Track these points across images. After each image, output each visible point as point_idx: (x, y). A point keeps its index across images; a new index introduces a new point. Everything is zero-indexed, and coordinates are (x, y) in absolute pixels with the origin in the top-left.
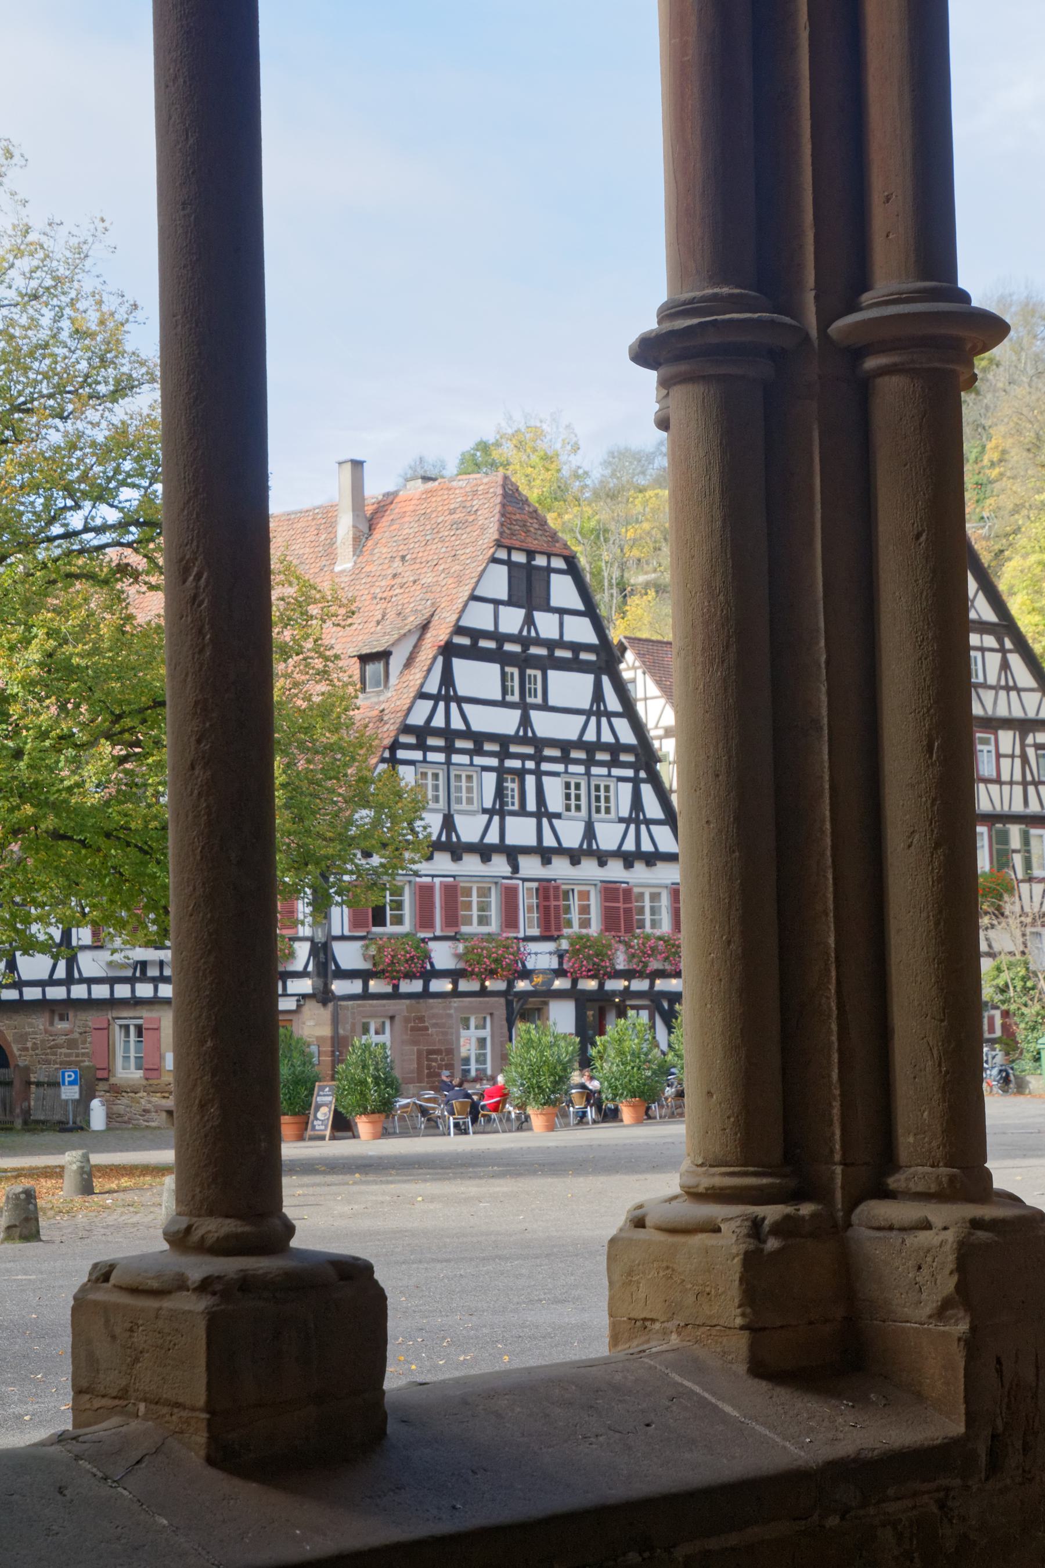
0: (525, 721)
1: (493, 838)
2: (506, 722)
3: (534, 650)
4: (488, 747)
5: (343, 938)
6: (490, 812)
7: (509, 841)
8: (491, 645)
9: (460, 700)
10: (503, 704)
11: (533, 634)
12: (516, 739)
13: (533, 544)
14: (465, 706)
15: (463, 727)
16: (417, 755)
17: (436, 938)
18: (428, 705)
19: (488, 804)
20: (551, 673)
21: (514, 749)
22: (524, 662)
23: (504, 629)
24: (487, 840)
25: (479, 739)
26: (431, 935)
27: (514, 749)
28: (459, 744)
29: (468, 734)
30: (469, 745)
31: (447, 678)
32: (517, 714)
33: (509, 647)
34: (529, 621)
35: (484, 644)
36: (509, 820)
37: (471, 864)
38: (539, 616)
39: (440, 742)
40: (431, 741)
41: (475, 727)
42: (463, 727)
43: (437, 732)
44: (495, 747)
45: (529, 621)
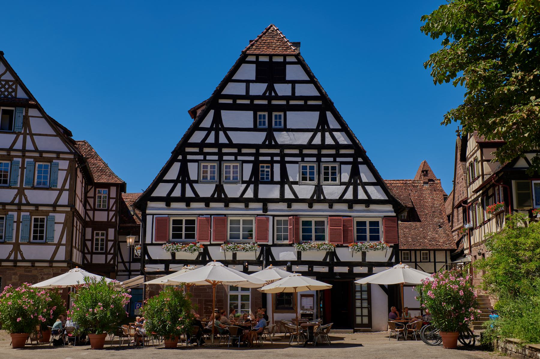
0: (270, 137)
1: (249, 194)
2: (259, 138)
3: (274, 102)
4: (244, 151)
5: (152, 244)
6: (248, 183)
7: (260, 196)
8: (248, 102)
9: (225, 130)
10: (255, 129)
11: (273, 94)
12: (263, 146)
13: (270, 51)
14: (229, 133)
15: (227, 142)
16: (201, 157)
17: (211, 245)
18: (204, 133)
19: (246, 177)
20: (288, 113)
21: (262, 151)
22: (270, 109)
23: (252, 93)
24: (245, 196)
25: (240, 146)
26: (209, 243)
27: (262, 151)
28: (225, 150)
29: (231, 145)
30: (235, 150)
31: (217, 119)
32: (264, 134)
33: (256, 102)
34: (271, 88)
35: (239, 102)
36: (261, 187)
37: (237, 209)
38: (277, 86)
39: (215, 150)
40: (206, 150)
41: (235, 142)
42: (227, 142)
43: (210, 145)
44: (253, 151)
45: (271, 88)
